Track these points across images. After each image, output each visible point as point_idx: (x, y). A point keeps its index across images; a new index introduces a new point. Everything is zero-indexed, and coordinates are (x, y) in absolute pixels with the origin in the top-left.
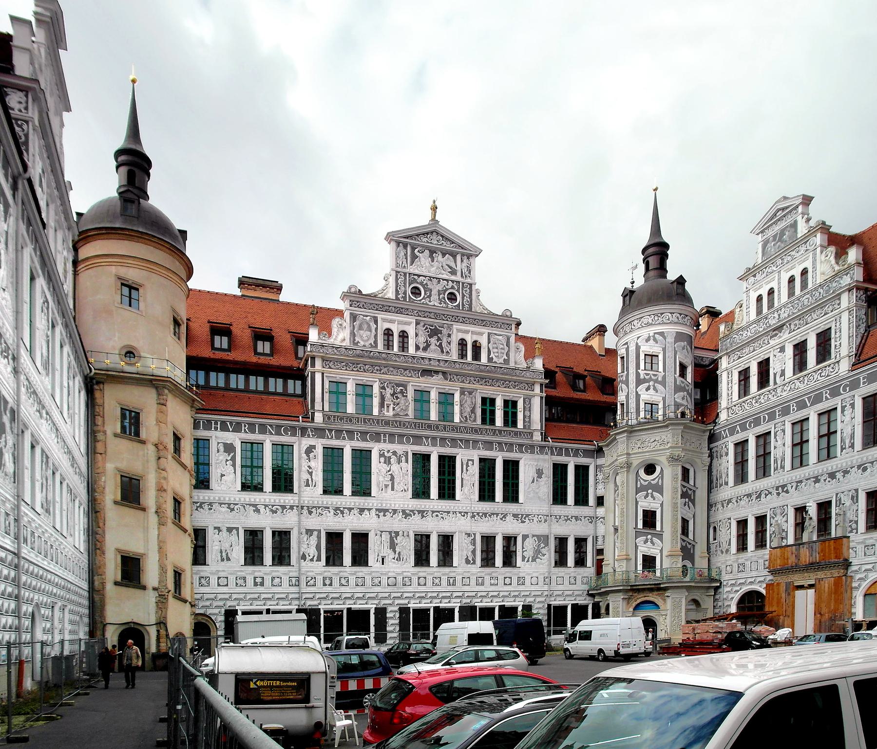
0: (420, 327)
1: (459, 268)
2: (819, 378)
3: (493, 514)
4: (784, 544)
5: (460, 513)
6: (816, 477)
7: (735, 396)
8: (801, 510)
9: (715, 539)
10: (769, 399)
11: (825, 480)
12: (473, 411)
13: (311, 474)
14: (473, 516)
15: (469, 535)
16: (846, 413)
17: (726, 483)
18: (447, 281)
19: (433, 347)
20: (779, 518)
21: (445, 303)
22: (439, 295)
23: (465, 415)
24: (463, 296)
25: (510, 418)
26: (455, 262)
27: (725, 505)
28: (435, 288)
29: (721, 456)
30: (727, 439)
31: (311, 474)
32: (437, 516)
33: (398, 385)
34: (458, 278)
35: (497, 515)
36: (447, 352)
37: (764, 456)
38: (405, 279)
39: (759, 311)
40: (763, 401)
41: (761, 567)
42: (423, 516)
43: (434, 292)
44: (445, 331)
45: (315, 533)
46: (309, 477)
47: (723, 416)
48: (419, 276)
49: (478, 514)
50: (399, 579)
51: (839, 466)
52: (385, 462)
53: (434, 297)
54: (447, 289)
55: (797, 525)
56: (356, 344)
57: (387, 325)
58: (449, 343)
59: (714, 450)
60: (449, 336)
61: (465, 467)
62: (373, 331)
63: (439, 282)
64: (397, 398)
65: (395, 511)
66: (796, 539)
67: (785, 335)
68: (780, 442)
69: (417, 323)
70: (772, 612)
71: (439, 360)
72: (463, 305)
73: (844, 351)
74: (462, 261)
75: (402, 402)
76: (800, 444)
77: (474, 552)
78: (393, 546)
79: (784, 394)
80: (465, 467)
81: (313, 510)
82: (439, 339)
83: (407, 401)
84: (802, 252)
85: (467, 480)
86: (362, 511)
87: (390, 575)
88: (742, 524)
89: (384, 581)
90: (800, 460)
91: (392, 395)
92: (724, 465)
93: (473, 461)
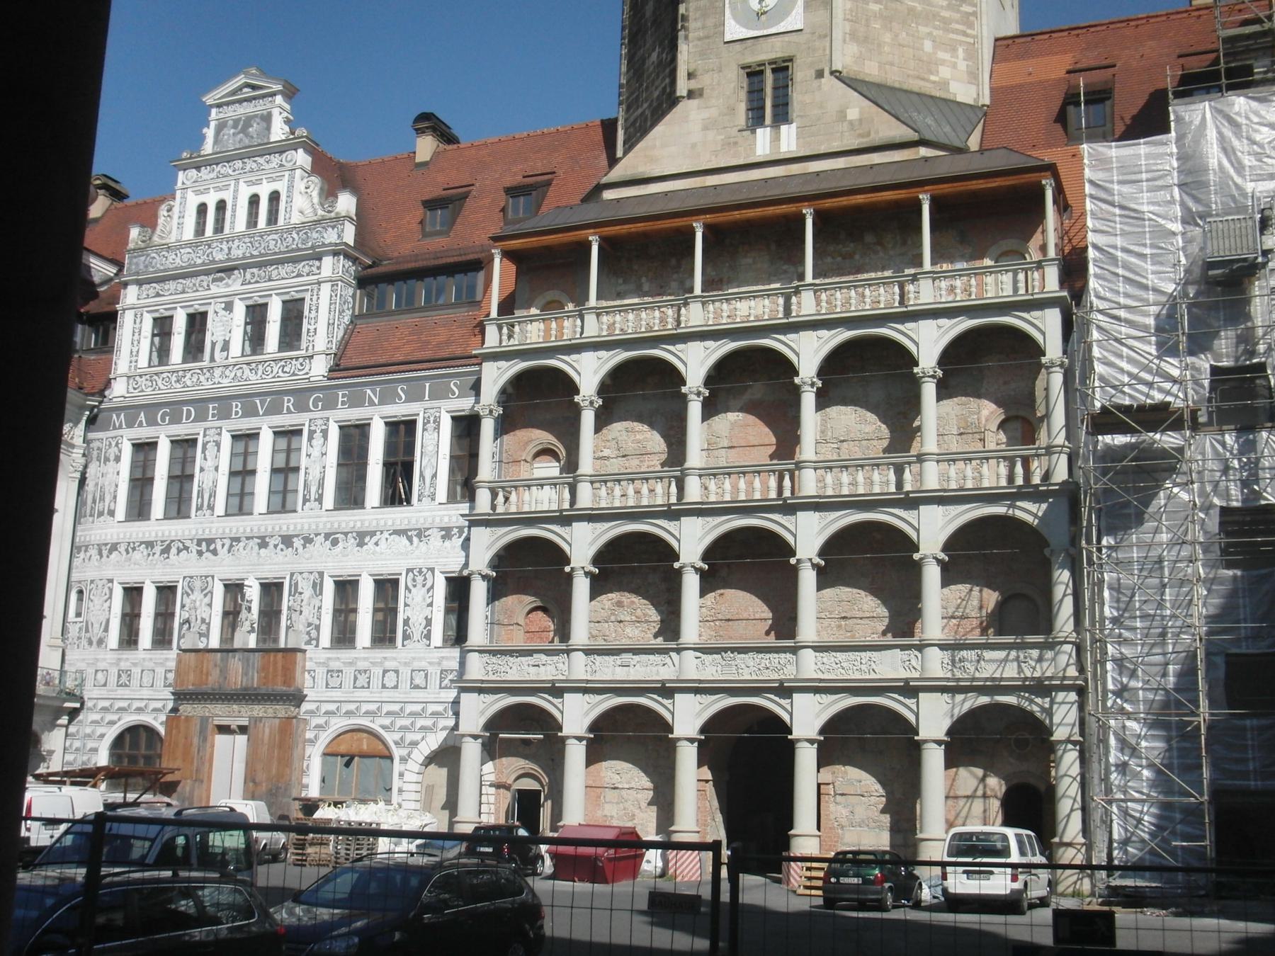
2: (281, 374)
4: (201, 646)
6: (263, 538)
7: (143, 361)
8: (234, 589)
9: (78, 615)
10: (199, 383)
11: (276, 546)
16: (314, 442)
17: (112, 513)
20: (197, 596)
27: (105, 553)
29: (107, 460)
30: (120, 432)
37: (181, 479)
39: (200, 230)
40: (189, 383)
41: (160, 683)
47: (119, 389)
51: (299, 527)
55: (226, 614)
59: (95, 445)
66: (222, 641)
67: (234, 284)
68: (210, 464)
70: (172, 771)
73: (321, 342)
76: (242, 474)
79: (224, 382)
84: (274, 165)
88: (133, 593)
90: (240, 503)
92: (111, 477)
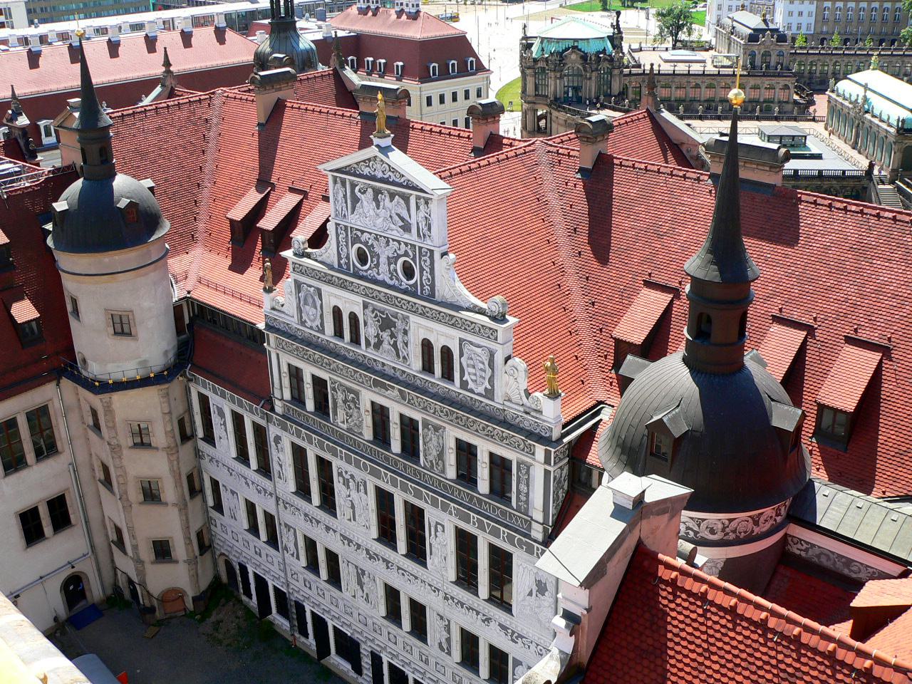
0: (368, 311)
1: (413, 221)
3: (473, 609)
5: (430, 585)
12: (441, 456)
13: (281, 466)
14: (446, 598)
15: (442, 618)
18: (399, 242)
19: (385, 346)
21: (397, 279)
22: (389, 264)
23: (430, 458)
24: (422, 270)
25: (500, 489)
26: (409, 210)
28: (385, 253)
31: (281, 466)
32: (403, 574)
33: (350, 390)
34: (412, 238)
35: (478, 613)
36: (404, 358)
38: (347, 235)
42: (388, 568)
43: (383, 260)
44: (399, 324)
45: (292, 530)
46: (279, 468)
48: (363, 232)
49: (453, 598)
50: (370, 622)
52: (344, 484)
53: (384, 267)
54: (399, 256)
56: (303, 323)
57: (335, 302)
58: (406, 344)
60: (406, 332)
61: (433, 529)
62: (319, 308)
63: (388, 242)
64: (350, 408)
65: (359, 546)
69: (365, 306)
71: (394, 368)
72: (422, 285)
74: (418, 208)
75: (355, 414)
77: (448, 640)
78: (360, 584)
80: (433, 529)
81: (287, 505)
82: (392, 336)
83: (360, 416)
85: (442, 547)
86: (328, 528)
87: (361, 612)
89: (355, 615)
91: (345, 401)
93: (443, 526)
